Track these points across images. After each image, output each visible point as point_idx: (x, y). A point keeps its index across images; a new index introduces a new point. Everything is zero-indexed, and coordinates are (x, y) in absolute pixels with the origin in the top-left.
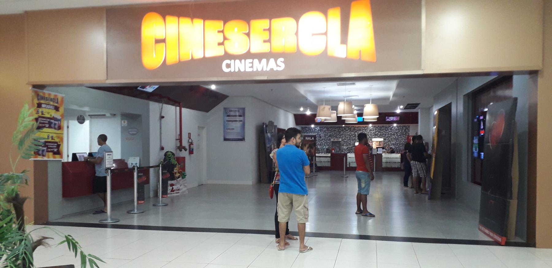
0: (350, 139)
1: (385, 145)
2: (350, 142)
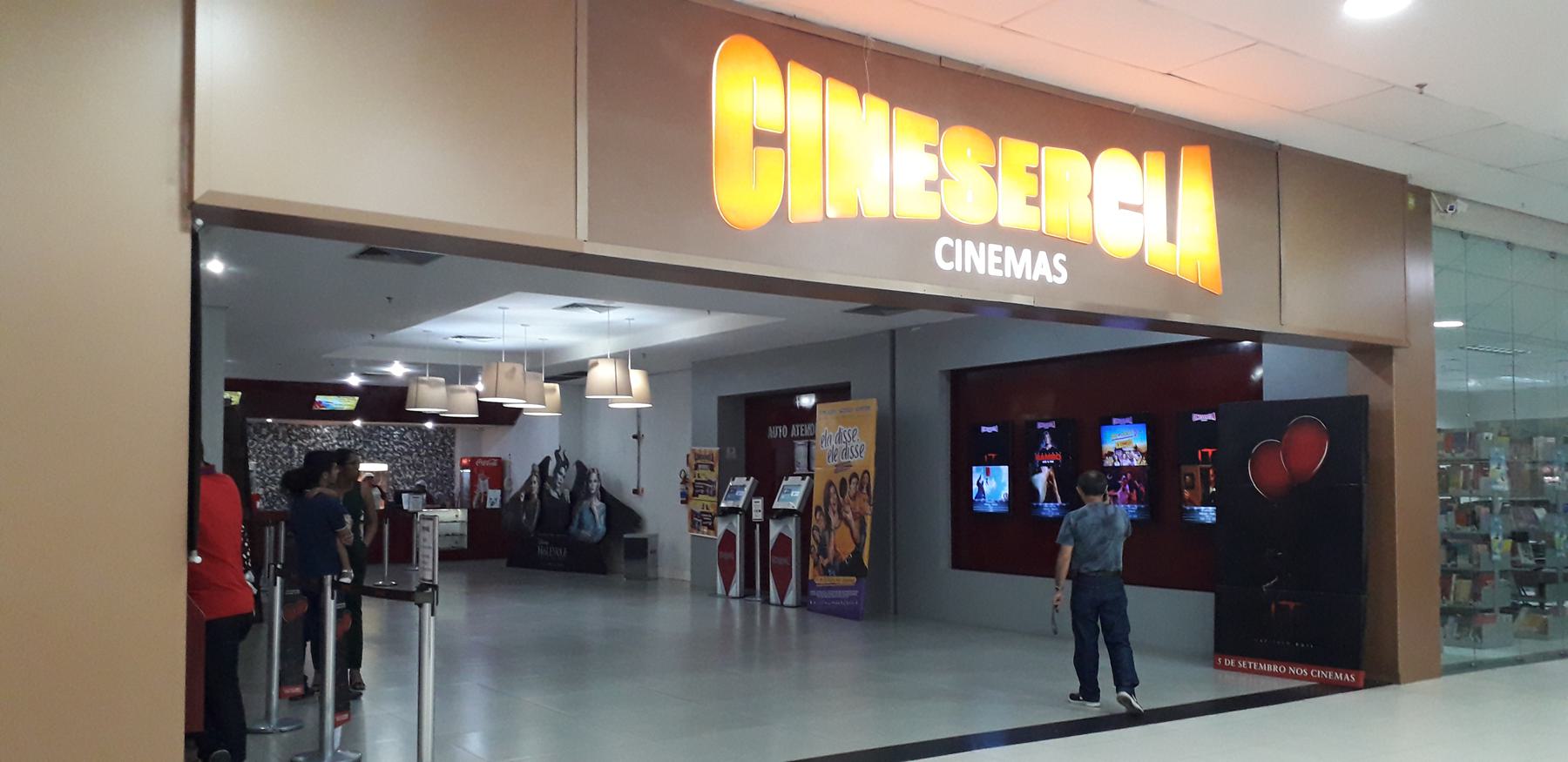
2: (274, 472)
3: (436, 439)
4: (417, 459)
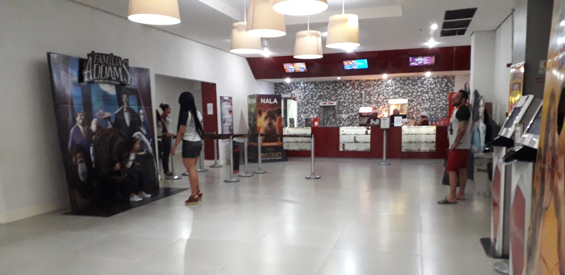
0: (352, 102)
1: (412, 110)
2: (352, 106)
3: (442, 83)
4: (432, 95)
